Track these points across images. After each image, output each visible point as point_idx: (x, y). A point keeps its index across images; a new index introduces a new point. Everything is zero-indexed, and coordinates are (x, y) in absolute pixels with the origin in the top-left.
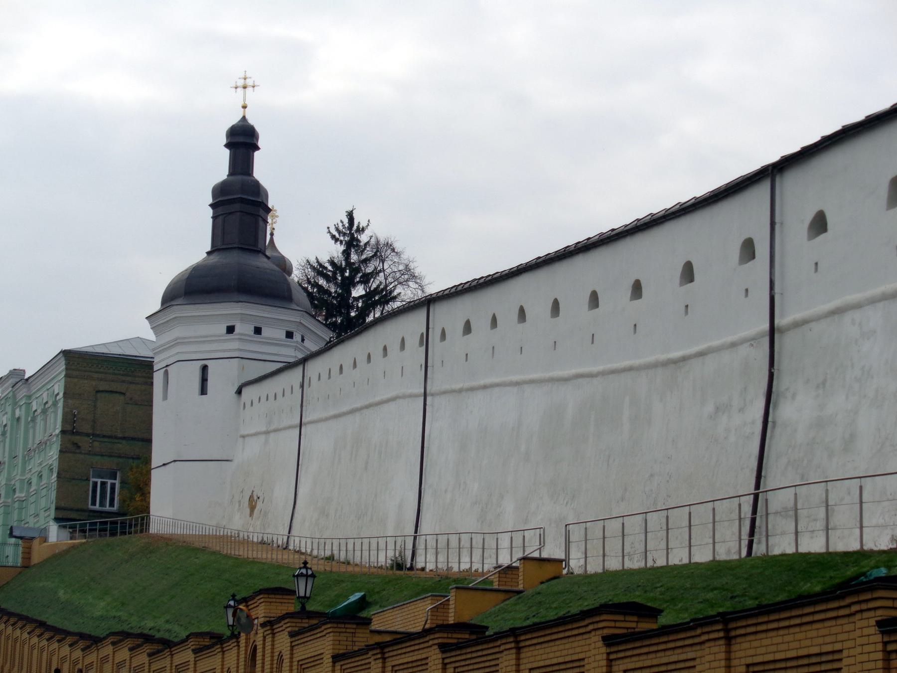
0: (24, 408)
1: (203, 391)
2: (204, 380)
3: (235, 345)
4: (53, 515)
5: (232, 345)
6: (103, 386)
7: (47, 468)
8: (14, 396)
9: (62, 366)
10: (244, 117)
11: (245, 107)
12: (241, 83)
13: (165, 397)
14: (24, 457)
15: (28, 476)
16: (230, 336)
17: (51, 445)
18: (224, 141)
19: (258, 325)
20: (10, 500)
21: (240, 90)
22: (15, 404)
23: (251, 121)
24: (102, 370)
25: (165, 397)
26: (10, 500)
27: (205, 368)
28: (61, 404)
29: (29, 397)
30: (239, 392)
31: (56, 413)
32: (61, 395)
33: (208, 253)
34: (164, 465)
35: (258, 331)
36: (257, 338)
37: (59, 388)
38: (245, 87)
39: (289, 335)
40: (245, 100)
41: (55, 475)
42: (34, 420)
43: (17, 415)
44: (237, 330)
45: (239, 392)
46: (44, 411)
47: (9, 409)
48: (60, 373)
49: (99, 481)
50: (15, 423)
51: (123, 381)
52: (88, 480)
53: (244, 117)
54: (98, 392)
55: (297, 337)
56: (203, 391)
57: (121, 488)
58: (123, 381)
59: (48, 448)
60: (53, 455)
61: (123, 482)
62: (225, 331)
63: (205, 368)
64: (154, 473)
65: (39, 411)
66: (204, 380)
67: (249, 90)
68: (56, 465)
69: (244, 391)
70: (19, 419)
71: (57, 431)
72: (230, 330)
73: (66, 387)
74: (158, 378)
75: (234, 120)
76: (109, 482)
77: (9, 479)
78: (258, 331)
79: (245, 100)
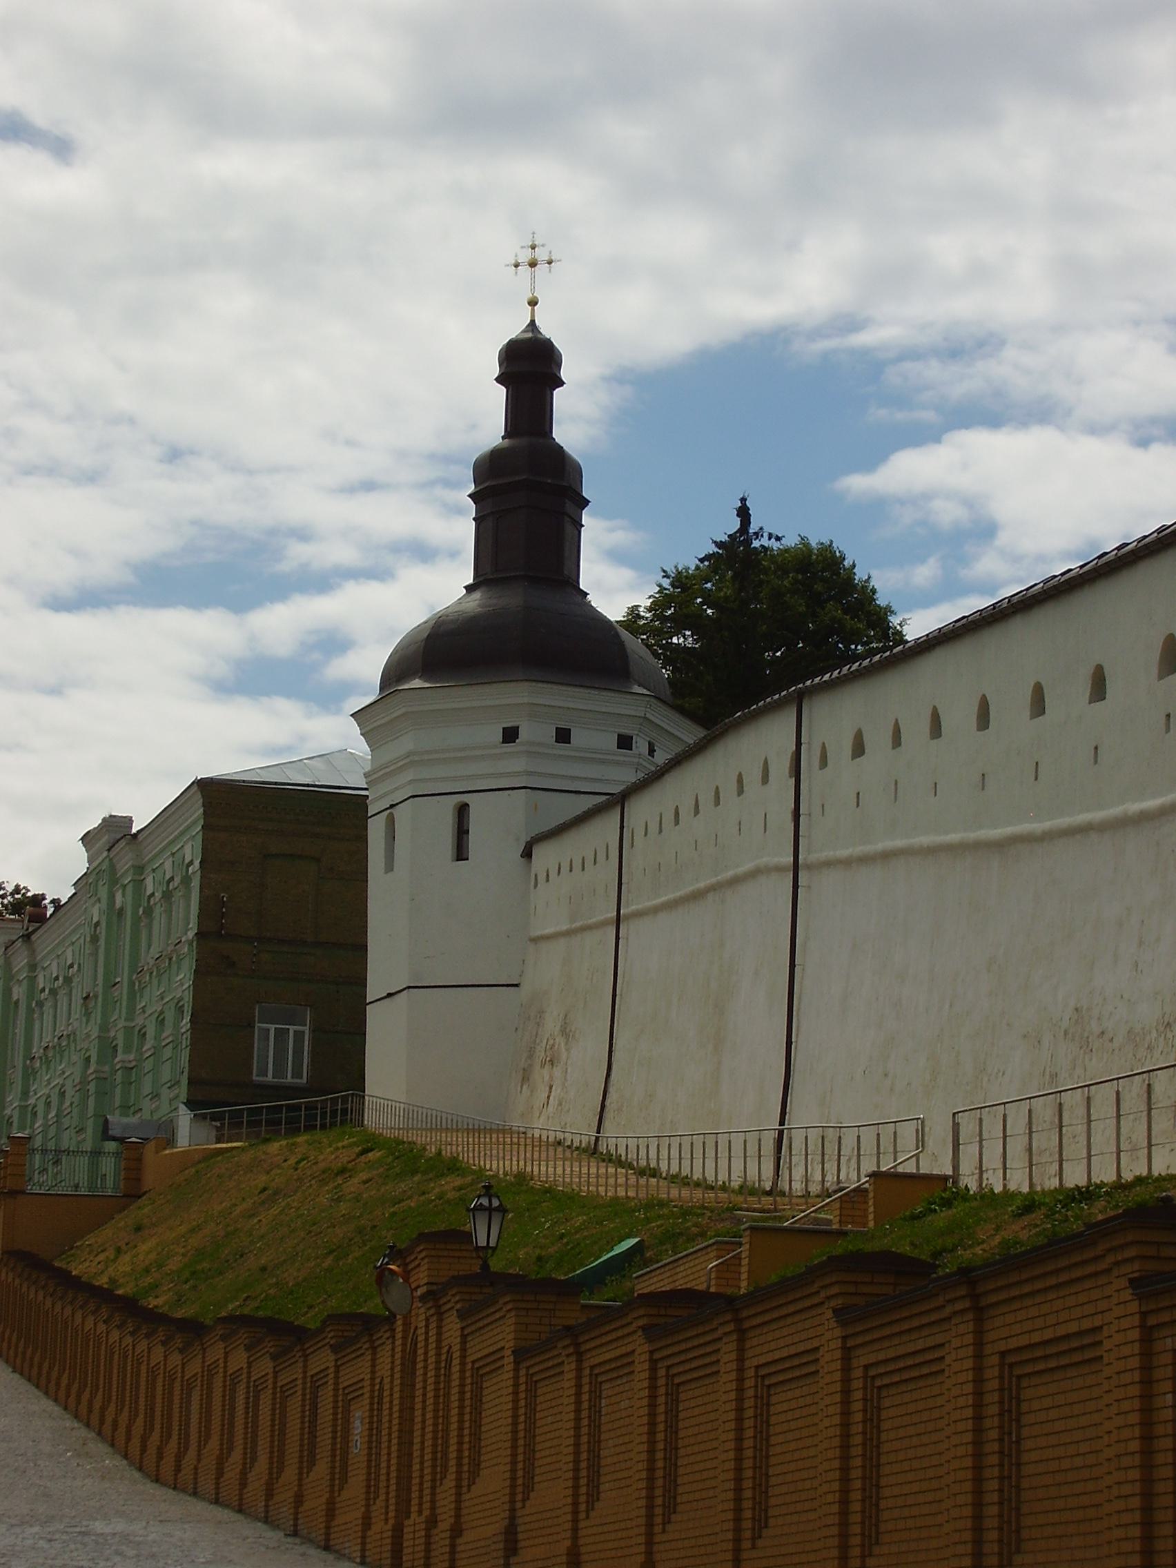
0: (129, 889)
1: (461, 853)
2: (462, 832)
3: (519, 764)
4: (184, 1096)
5: (514, 764)
7: (173, 1005)
8: (113, 868)
9: (197, 811)
10: (533, 323)
11: (533, 303)
12: (525, 256)
13: (389, 867)
14: (131, 984)
15: (139, 1021)
16: (510, 747)
17: (180, 960)
18: (496, 371)
20: (107, 1068)
21: (524, 270)
22: (114, 881)
25: (389, 867)
26: (107, 1068)
27: (462, 811)
28: (196, 883)
29: (139, 869)
30: (527, 854)
31: (187, 898)
32: (197, 863)
33: (469, 589)
34: (390, 995)
35: (563, 736)
37: (192, 851)
38: (533, 264)
39: (625, 742)
40: (533, 290)
41: (187, 1019)
42: (149, 912)
43: (118, 904)
44: (523, 734)
45: (527, 854)
46: (167, 895)
47: (103, 893)
48: (195, 823)
49: (272, 1027)
50: (115, 918)
52: (251, 1025)
53: (533, 323)
55: (641, 746)
56: (461, 853)
57: (315, 1042)
59: (174, 967)
60: (182, 980)
61: (314, 1031)
63: (462, 811)
64: (374, 1015)
65: (158, 895)
66: (462, 832)
67: (541, 269)
68: (188, 999)
69: (536, 851)
70: (121, 912)
71: (191, 934)
72: (510, 735)
73: (205, 850)
74: (376, 830)
75: (514, 329)
76: (292, 1028)
77: (104, 1028)
78: (563, 736)
79: (533, 290)
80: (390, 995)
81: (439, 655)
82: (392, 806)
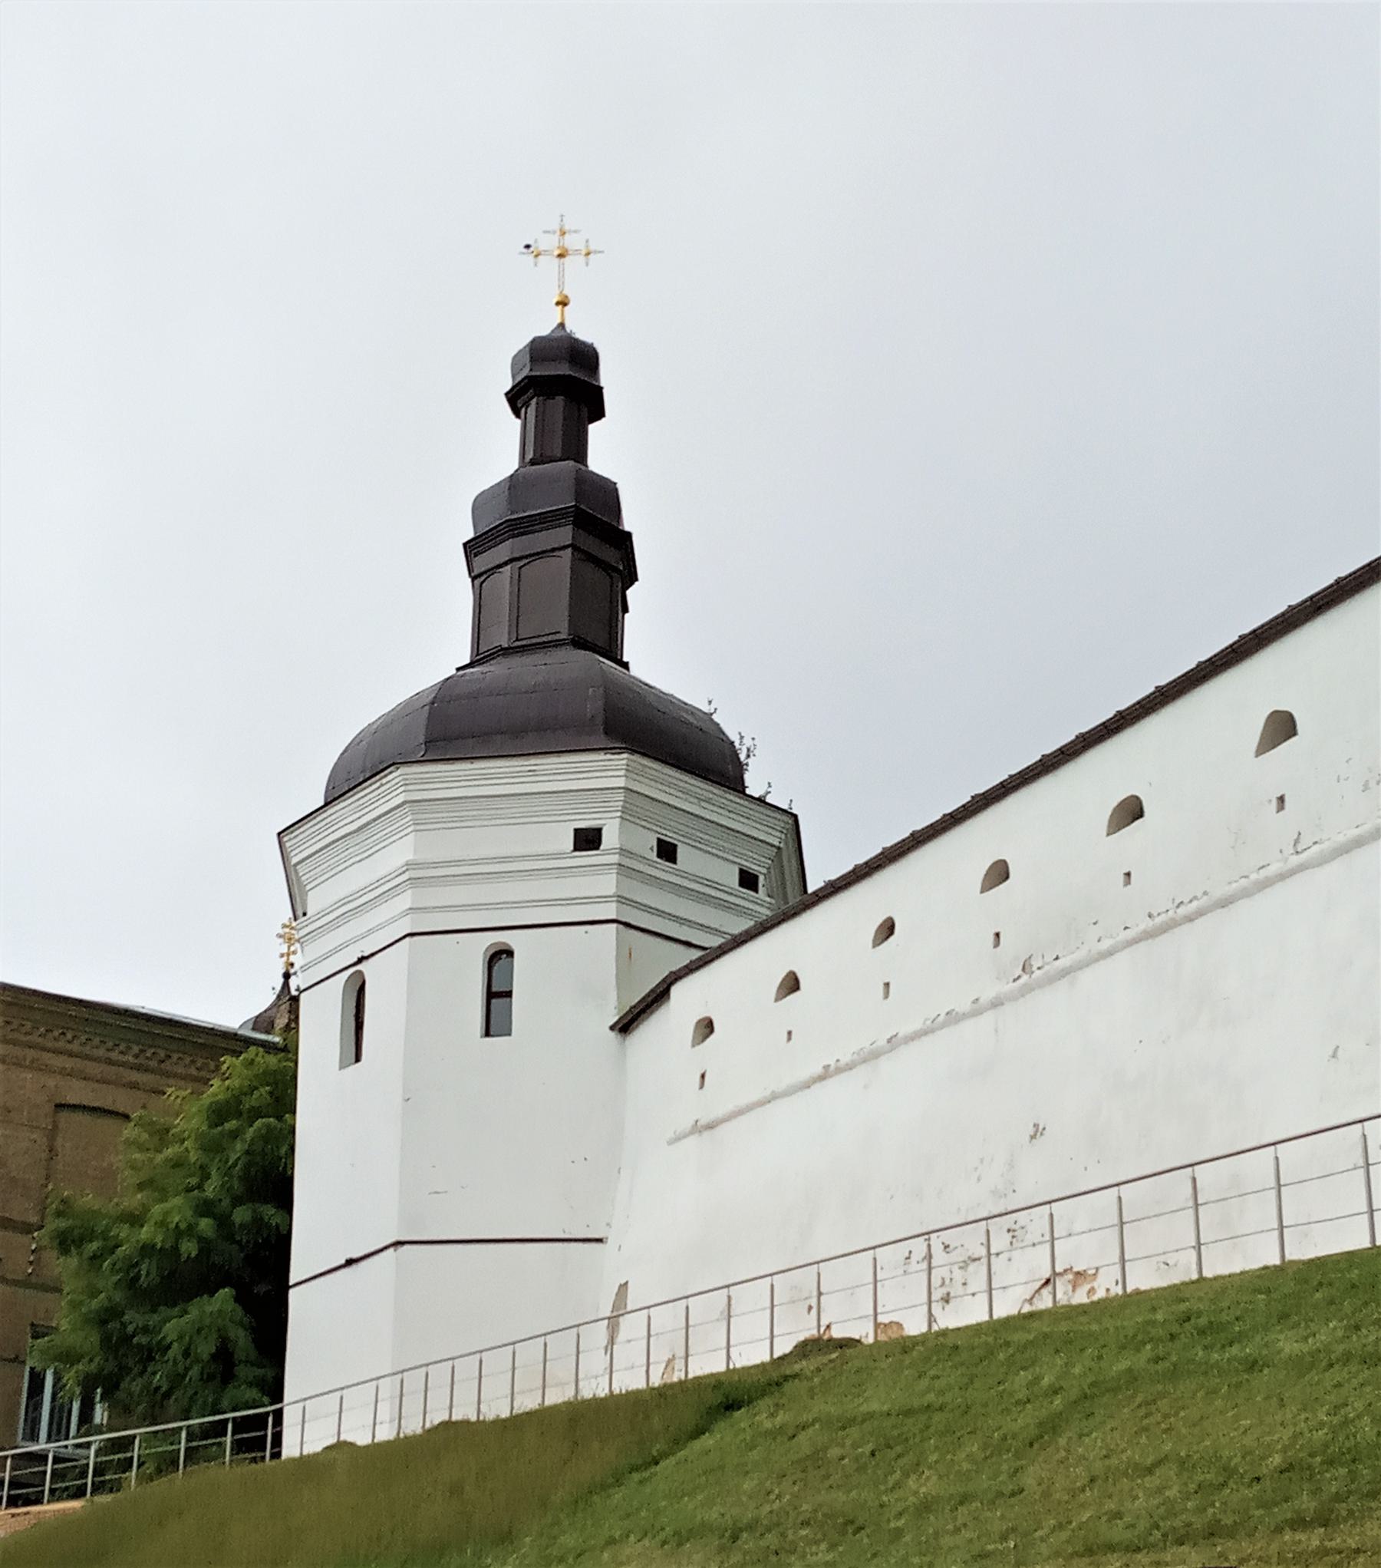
1: (494, 1024)
2: (497, 995)
5: (597, 882)
6: (77, 1093)
10: (562, 325)
11: (563, 303)
16: (588, 857)
19: (670, 837)
21: (549, 263)
23: (582, 331)
24: (75, 1047)
27: (500, 956)
33: (458, 669)
34: (350, 1262)
35: (667, 851)
36: (662, 870)
39: (748, 880)
44: (609, 839)
51: (134, 1086)
53: (562, 325)
54: (60, 1106)
56: (494, 1024)
58: (134, 1086)
62: (570, 844)
63: (500, 956)
66: (497, 995)
72: (588, 840)
78: (667, 851)
80: (350, 1262)
81: (450, 728)
82: (360, 960)
